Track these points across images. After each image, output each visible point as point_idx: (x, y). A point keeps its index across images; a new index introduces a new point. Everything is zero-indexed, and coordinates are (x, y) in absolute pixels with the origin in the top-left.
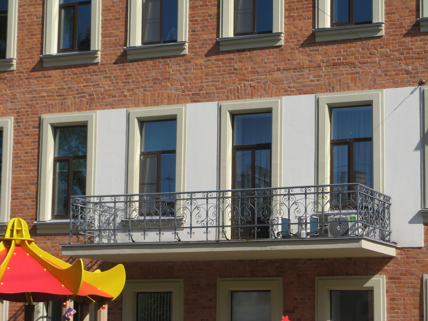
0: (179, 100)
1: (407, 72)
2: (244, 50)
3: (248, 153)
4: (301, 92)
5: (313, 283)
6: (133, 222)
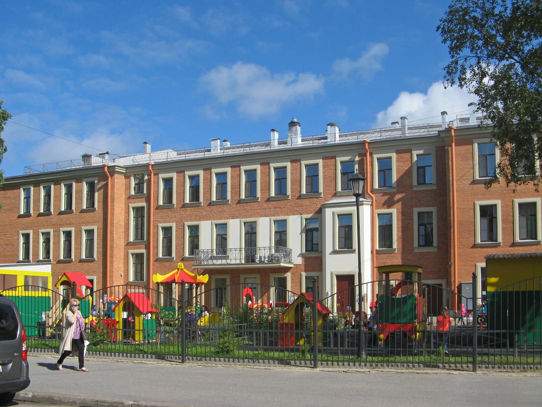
0: (228, 218)
1: (297, 211)
2: (248, 203)
3: (249, 235)
4: (265, 216)
5: (269, 275)
6: (215, 256)
